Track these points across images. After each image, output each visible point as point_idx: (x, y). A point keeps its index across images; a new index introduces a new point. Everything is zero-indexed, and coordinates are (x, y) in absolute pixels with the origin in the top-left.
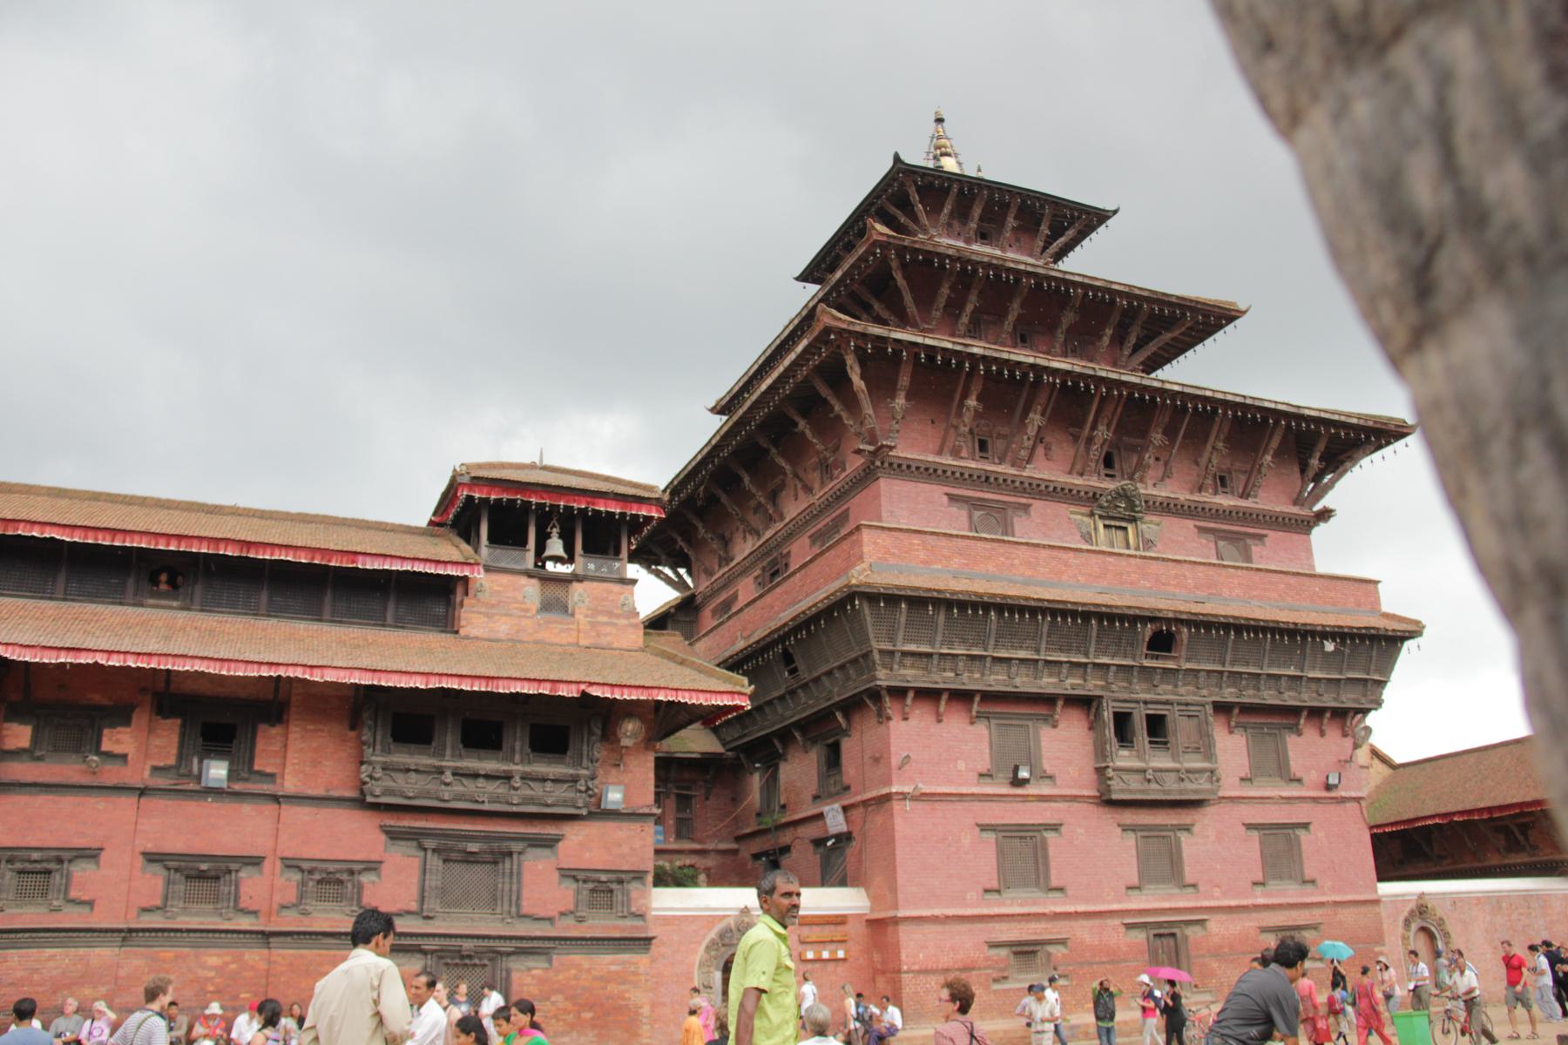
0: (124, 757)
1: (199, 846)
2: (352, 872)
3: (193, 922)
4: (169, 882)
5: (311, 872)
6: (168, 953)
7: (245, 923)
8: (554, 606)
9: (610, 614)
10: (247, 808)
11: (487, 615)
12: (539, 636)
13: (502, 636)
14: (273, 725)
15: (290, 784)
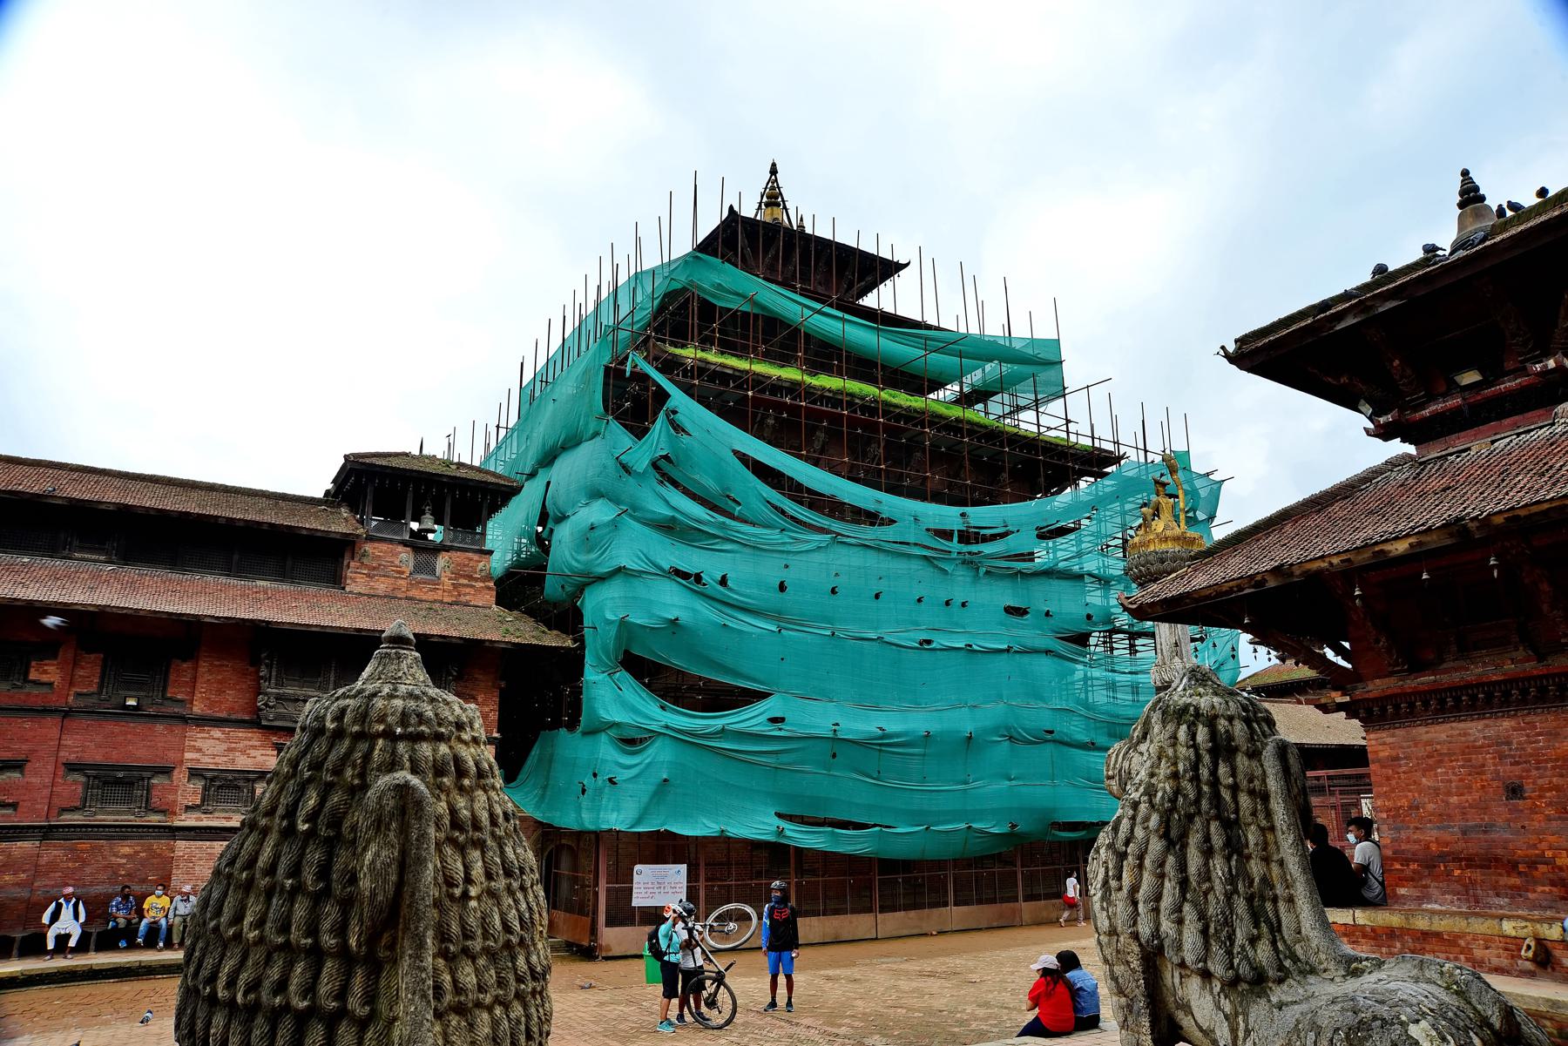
0: (51, 684)
1: (116, 757)
2: (248, 780)
3: (109, 819)
4: (87, 787)
5: (213, 779)
6: (85, 845)
7: (154, 819)
8: (425, 568)
9: (470, 578)
10: (159, 728)
11: (368, 575)
12: (410, 594)
13: (380, 593)
14: (184, 661)
15: (198, 708)
